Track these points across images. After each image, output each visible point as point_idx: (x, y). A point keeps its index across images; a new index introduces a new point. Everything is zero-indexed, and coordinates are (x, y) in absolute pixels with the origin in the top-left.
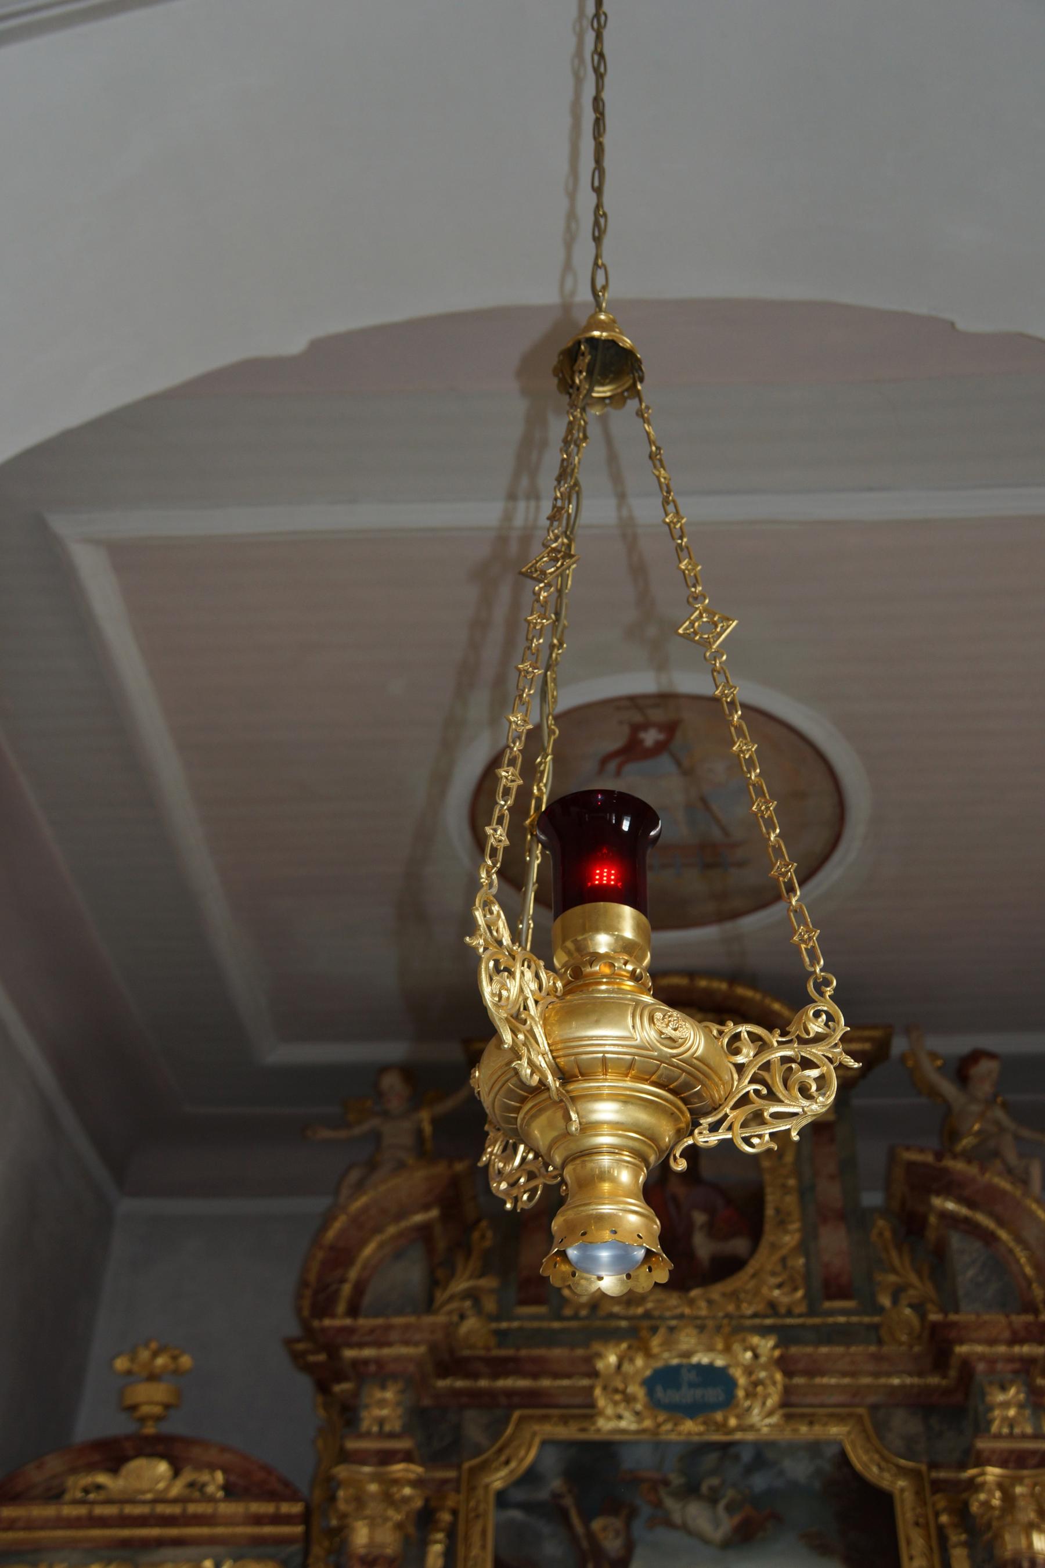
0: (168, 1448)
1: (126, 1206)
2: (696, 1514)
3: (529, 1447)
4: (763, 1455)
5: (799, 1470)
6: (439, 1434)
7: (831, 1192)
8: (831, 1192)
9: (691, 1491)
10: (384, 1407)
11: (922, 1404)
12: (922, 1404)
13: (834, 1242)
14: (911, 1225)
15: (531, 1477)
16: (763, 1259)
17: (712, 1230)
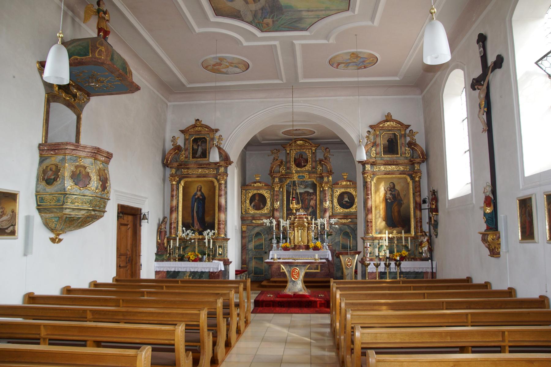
0: (260, 182)
1: (247, 152)
2: (302, 186)
3: (288, 181)
4: (307, 182)
5: (310, 183)
6: (281, 181)
7: (314, 159)
8: (314, 159)
9: (301, 184)
10: (277, 180)
11: (320, 177)
12: (320, 177)
13: (314, 164)
14: (320, 163)
15: (289, 184)
16: (308, 165)
17: (304, 163)
